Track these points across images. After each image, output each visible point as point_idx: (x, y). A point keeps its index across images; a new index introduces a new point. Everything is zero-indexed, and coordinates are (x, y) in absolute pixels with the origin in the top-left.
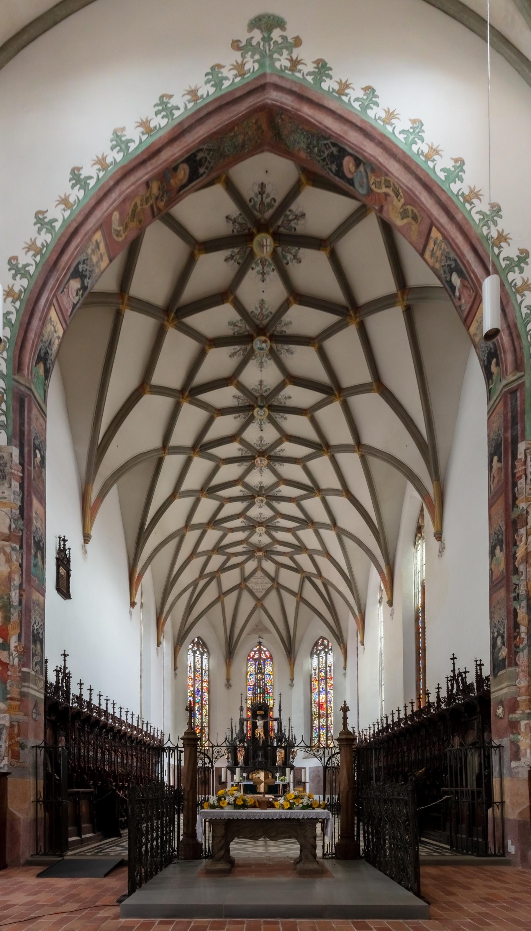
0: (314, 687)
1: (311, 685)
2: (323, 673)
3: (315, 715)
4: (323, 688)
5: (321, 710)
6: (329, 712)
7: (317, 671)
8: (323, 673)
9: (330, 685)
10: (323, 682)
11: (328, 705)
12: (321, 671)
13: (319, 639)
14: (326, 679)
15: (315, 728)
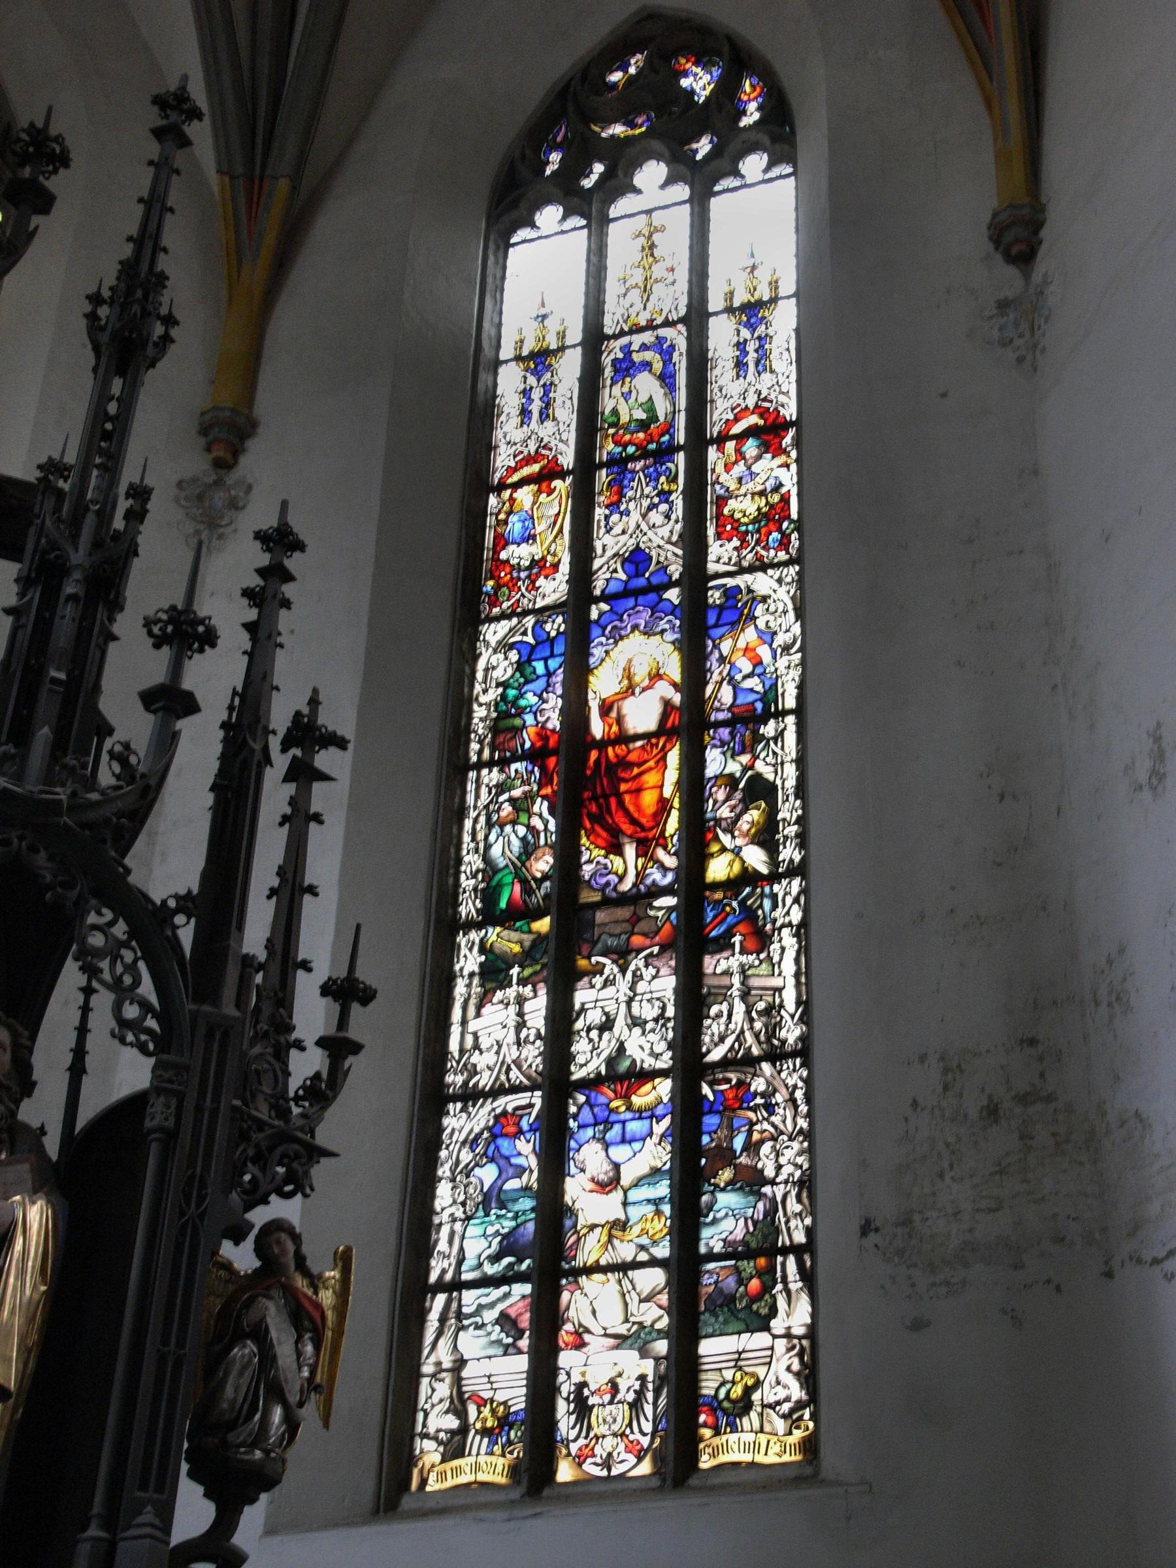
0: (518, 554)
1: (475, 517)
2: (646, 385)
3: (490, 916)
4: (637, 559)
5: (592, 857)
6: (718, 869)
7: (569, 368)
8: (646, 385)
9: (745, 507)
10: (640, 489)
11: (715, 762)
12: (626, 368)
13: (616, 55)
14: (698, 442)
15: (482, 1116)
